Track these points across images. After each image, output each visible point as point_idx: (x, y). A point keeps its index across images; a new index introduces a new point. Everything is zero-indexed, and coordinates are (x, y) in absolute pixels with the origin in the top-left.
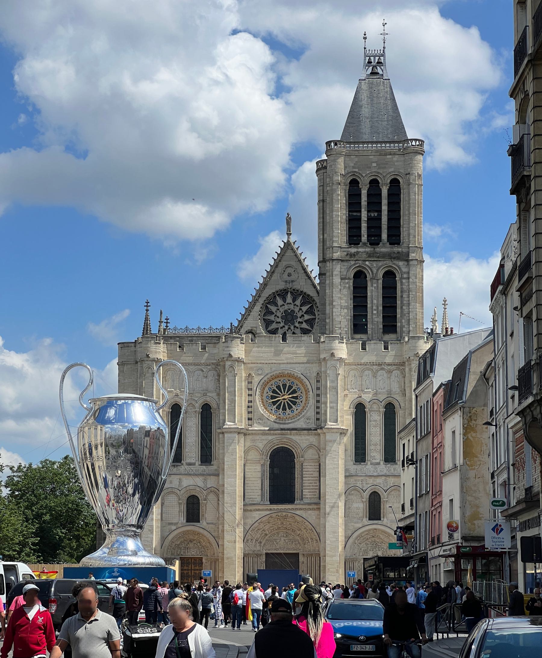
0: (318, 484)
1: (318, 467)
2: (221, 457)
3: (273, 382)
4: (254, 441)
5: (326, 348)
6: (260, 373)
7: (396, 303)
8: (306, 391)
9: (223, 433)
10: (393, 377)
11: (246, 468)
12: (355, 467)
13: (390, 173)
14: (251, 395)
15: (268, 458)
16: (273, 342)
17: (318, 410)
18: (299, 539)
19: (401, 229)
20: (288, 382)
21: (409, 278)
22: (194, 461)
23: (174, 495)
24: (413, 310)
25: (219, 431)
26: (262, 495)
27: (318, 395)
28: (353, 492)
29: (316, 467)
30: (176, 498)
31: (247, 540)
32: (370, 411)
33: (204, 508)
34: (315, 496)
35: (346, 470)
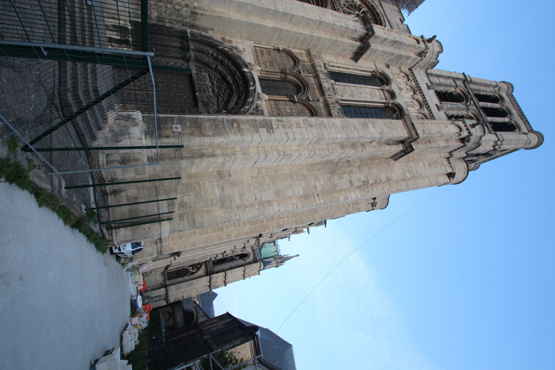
28: (290, 59)
32: (383, 90)
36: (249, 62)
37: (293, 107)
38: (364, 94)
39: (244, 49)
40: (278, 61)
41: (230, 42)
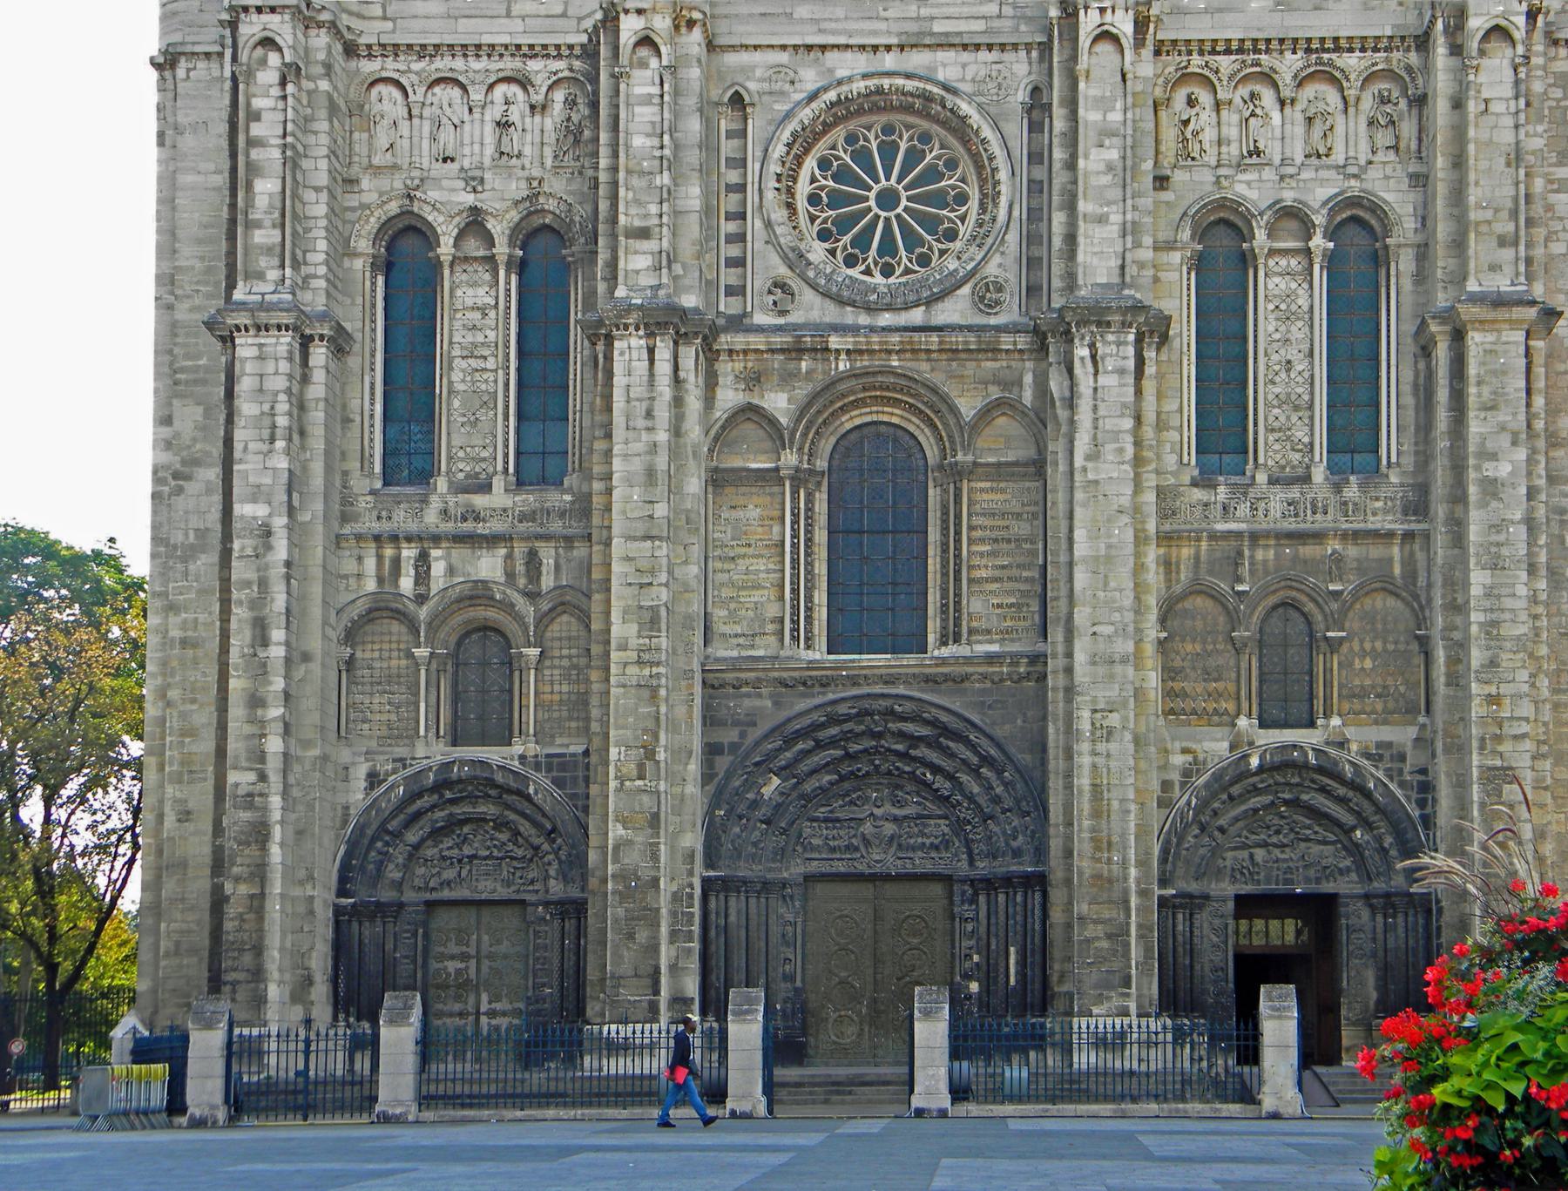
3: (839, 134)
8: (979, 167)
23: (396, 627)
28: (1188, 604)
36: (1226, 745)
37: (1356, 646)
38: (1292, 353)
39: (1185, 751)
40: (1198, 648)
41: (1166, 785)
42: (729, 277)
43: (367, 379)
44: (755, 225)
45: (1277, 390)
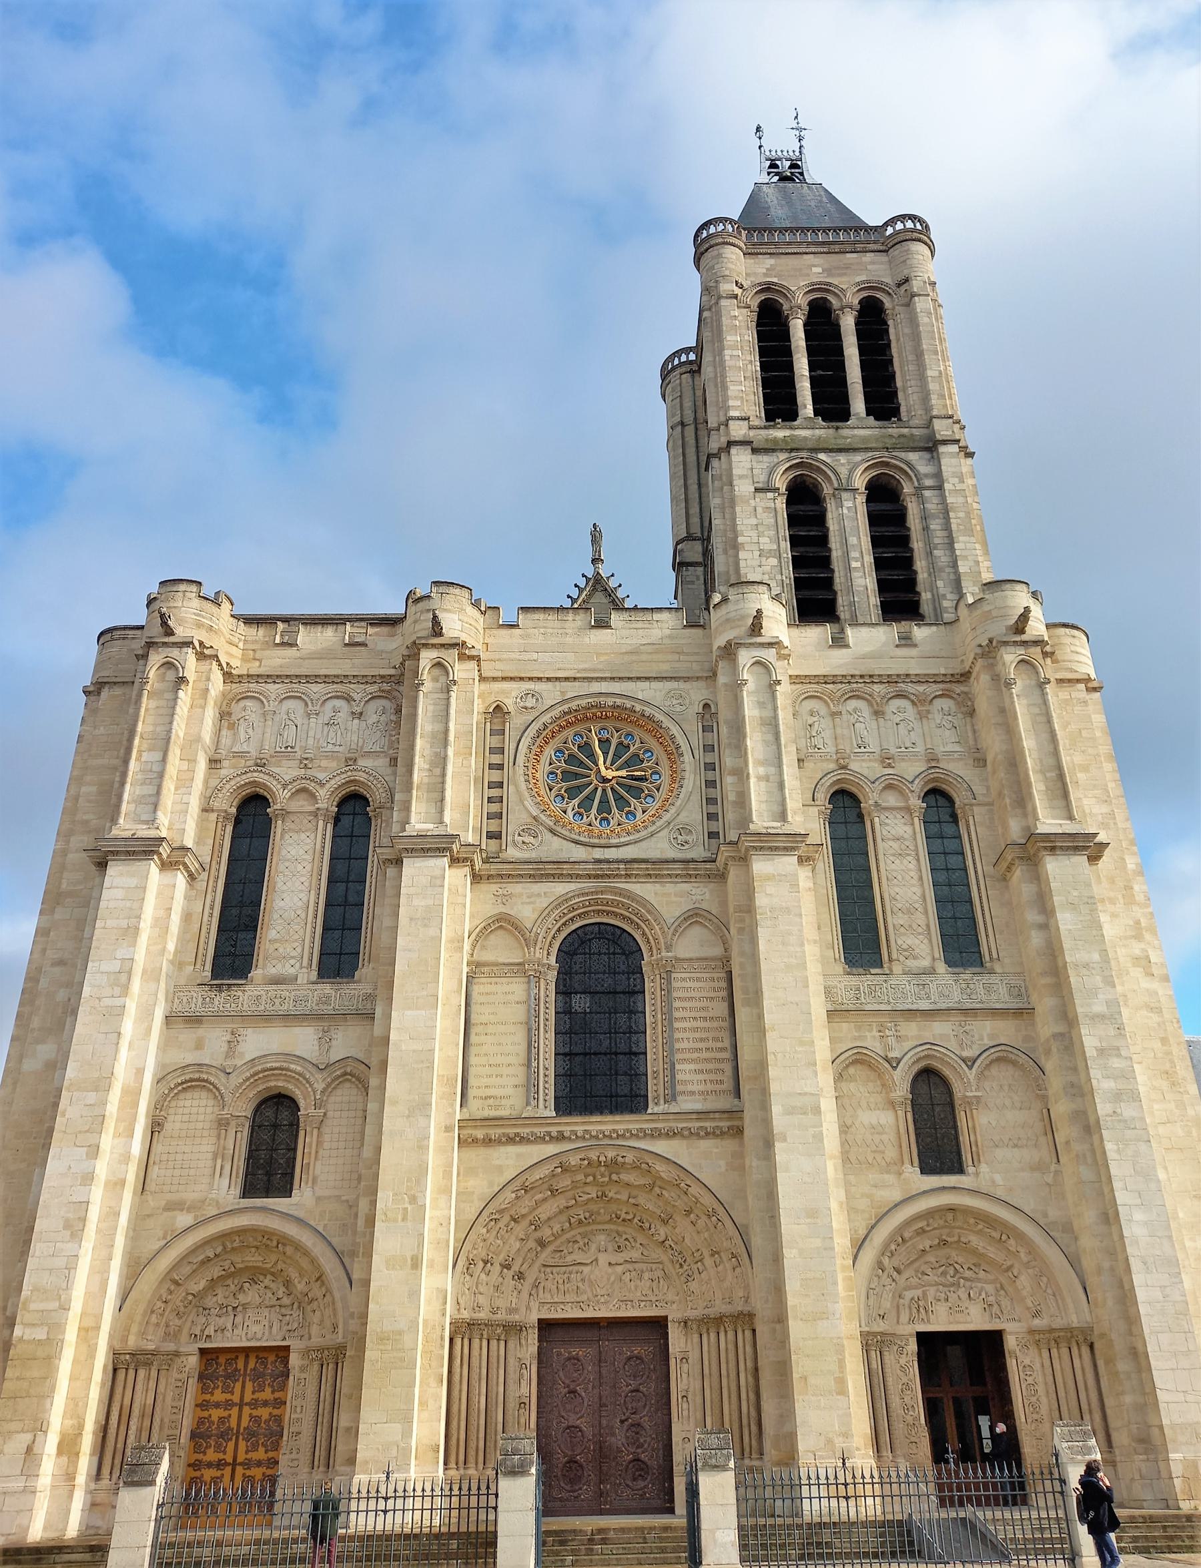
0: (727, 1043)
1: (724, 985)
2: (385, 939)
3: (569, 733)
4: (505, 898)
5: (732, 615)
6: (529, 705)
7: (912, 550)
8: (669, 754)
9: (399, 862)
10: (938, 718)
11: (476, 989)
12: (853, 981)
13: (858, 284)
14: (500, 767)
15: (553, 959)
16: (567, 625)
17: (712, 809)
18: (664, 1258)
19: (900, 395)
20: (616, 735)
21: (940, 488)
22: (292, 971)
24: (964, 553)
25: (386, 853)
26: (531, 1087)
27: (710, 767)
28: (851, 1070)
29: (716, 984)
30: (211, 1102)
31: (471, 1262)
33: (311, 1139)
34: (718, 1087)
35: (828, 991)
42: (494, 826)
43: (209, 897)
44: (510, 793)
45: (900, 906)
